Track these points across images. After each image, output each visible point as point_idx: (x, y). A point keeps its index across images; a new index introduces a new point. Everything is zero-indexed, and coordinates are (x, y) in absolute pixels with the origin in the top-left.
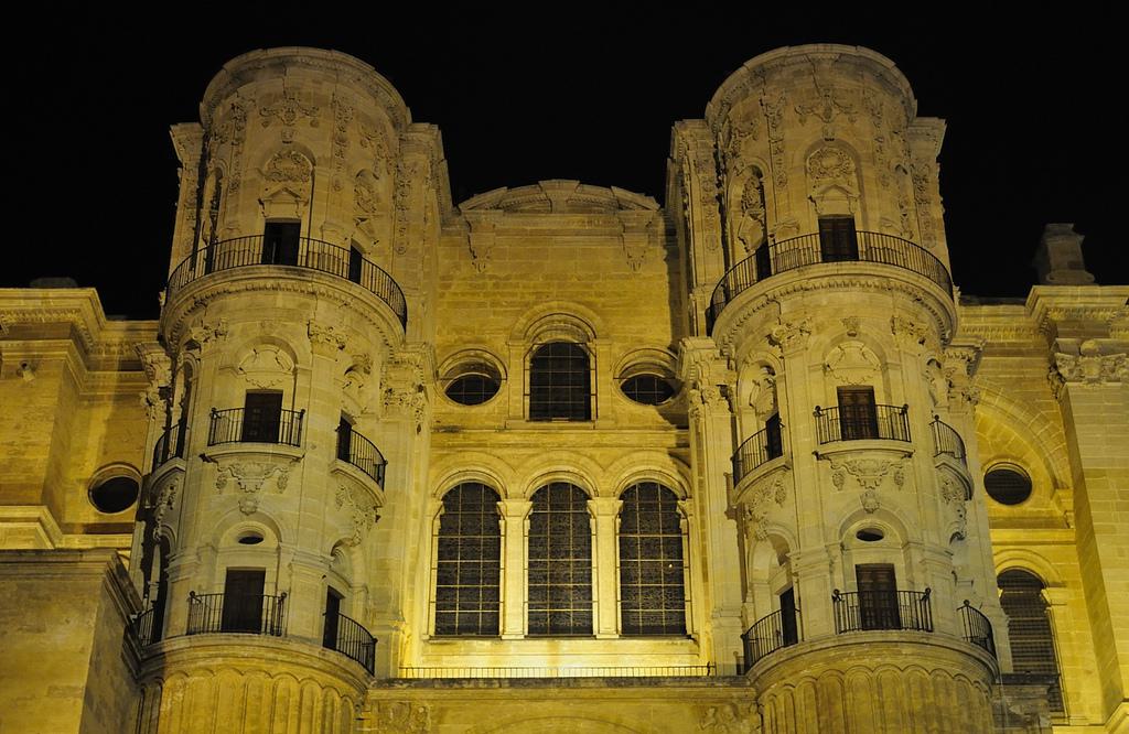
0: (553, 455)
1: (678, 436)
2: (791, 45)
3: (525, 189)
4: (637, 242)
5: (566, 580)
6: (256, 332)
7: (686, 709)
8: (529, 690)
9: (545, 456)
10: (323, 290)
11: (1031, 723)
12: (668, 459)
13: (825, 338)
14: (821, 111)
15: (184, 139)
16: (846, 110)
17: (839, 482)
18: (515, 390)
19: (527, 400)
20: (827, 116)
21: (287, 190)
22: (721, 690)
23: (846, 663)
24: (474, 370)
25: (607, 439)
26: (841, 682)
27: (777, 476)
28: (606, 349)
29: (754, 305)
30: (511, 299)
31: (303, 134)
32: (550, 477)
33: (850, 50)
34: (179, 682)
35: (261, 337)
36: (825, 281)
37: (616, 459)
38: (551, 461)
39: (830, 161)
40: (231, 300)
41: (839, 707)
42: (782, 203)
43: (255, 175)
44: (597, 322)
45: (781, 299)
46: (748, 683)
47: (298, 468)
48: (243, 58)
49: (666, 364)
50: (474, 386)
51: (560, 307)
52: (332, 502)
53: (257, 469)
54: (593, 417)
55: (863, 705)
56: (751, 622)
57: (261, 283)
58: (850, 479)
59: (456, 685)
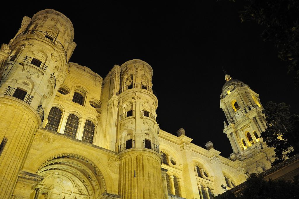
0: (76, 109)
1: (99, 115)
2: (141, 60)
3: (82, 66)
4: (97, 83)
5: (71, 131)
6: (41, 48)
7: (106, 156)
8: (75, 142)
9: (74, 108)
12: (96, 118)
13: (143, 101)
15: (26, 21)
17: (144, 123)
18: (71, 95)
21: (52, 32)
22: (113, 155)
23: (144, 154)
24: (62, 90)
25: (86, 110)
28: (89, 96)
29: (130, 92)
31: (58, 26)
32: (73, 112)
33: (149, 65)
35: (41, 50)
36: (145, 92)
37: (87, 114)
38: (75, 110)
40: (36, 41)
42: (137, 79)
43: (47, 27)
44: (88, 91)
45: (136, 93)
46: (119, 155)
47: (42, 76)
48: (51, 10)
49: (97, 103)
50: (63, 91)
51: (82, 86)
54: (84, 105)
55: (146, 162)
57: (45, 41)
59: (60, 135)
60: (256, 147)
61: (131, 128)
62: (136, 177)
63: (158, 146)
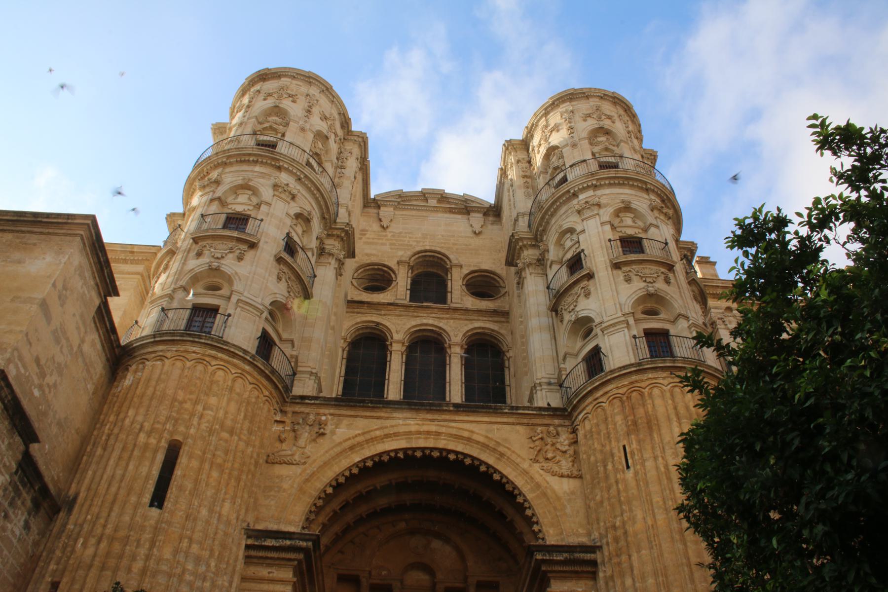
10: (285, 166)
13: (611, 210)
16: (609, 117)
17: (628, 280)
19: (408, 292)
20: (599, 119)
26: (642, 395)
27: (584, 283)
30: (401, 243)
31: (286, 104)
34: (141, 366)
39: (603, 139)
41: (640, 412)
52: (275, 277)
53: (225, 247)
54: (449, 301)
56: (564, 377)
58: (635, 278)
62: (632, 469)
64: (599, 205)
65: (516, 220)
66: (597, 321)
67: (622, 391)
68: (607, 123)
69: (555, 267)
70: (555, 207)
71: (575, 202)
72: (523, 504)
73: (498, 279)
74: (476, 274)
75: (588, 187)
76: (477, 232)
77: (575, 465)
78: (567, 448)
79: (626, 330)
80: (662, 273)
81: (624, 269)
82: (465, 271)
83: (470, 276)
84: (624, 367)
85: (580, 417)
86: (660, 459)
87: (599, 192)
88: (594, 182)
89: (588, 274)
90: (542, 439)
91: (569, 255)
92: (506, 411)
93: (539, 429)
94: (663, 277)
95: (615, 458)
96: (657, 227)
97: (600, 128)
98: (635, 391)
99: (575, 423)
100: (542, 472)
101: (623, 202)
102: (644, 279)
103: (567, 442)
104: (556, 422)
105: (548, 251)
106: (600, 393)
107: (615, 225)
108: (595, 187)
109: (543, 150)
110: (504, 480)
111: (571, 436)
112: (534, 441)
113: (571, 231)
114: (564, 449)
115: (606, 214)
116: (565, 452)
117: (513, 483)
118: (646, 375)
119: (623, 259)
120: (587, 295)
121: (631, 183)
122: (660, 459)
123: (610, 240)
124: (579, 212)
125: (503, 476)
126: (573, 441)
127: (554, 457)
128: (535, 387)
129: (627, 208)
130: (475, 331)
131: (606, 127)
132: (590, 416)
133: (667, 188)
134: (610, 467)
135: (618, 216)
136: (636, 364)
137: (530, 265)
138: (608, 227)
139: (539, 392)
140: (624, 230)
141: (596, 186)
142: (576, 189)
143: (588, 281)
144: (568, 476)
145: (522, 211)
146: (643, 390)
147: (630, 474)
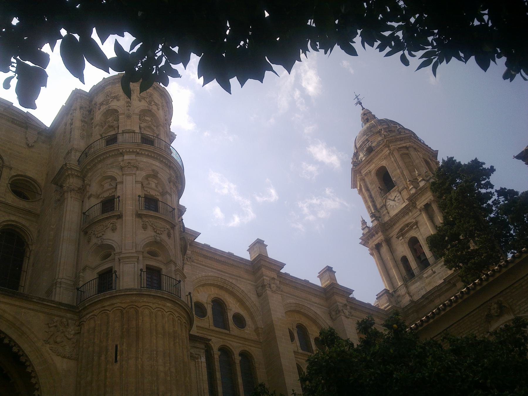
11: (197, 358)
13: (144, 174)
14: (147, 100)
17: (145, 228)
20: (150, 103)
26: (137, 312)
27: (114, 220)
56: (81, 284)
60: (434, 272)
61: (109, 242)
62: (119, 363)
63: (180, 282)
64: (137, 168)
65: (69, 153)
66: (117, 250)
67: (123, 306)
68: (154, 108)
69: (94, 201)
70: (105, 157)
71: (120, 159)
72: (31, 373)
73: (37, 187)
74: (21, 178)
75: (133, 152)
76: (30, 145)
77: (75, 350)
78: (72, 336)
79: (136, 264)
80: (167, 229)
81: (144, 219)
82: (13, 173)
83: (16, 178)
84: (130, 290)
85: (88, 316)
86: (140, 360)
87: (139, 158)
88: (138, 151)
89: (119, 215)
90: (56, 326)
91: (106, 195)
92: (35, 300)
93: (56, 319)
94: (167, 231)
95: (109, 353)
96: (170, 195)
97: (149, 110)
98: (133, 307)
99: (82, 320)
100: (50, 351)
101: (153, 170)
102: (155, 230)
103: (73, 332)
104: (69, 315)
105: (90, 185)
106: (108, 303)
107: (144, 185)
108: (138, 154)
109: (104, 108)
110: (21, 353)
111: (77, 328)
112: (49, 327)
113: (113, 178)
114: (70, 337)
115: (141, 175)
116: (70, 339)
117: (27, 356)
118: (143, 298)
119: (145, 212)
120: (114, 230)
121: (161, 159)
122: (140, 360)
123: (139, 196)
124: (122, 168)
125: (20, 349)
126: (77, 332)
127: (63, 342)
128: (56, 284)
129: (155, 175)
130: (9, 223)
131: (153, 111)
132: (95, 317)
133: (179, 165)
134: (103, 358)
135: (147, 179)
136: (138, 289)
137: (73, 190)
138: (139, 186)
139: (58, 289)
140: (149, 190)
141: (138, 153)
142: (124, 151)
143: (117, 220)
144: (69, 358)
145: (75, 147)
146: (138, 309)
147: (117, 366)
